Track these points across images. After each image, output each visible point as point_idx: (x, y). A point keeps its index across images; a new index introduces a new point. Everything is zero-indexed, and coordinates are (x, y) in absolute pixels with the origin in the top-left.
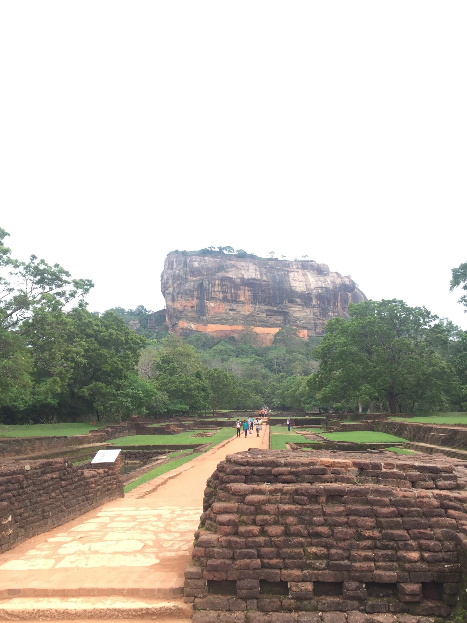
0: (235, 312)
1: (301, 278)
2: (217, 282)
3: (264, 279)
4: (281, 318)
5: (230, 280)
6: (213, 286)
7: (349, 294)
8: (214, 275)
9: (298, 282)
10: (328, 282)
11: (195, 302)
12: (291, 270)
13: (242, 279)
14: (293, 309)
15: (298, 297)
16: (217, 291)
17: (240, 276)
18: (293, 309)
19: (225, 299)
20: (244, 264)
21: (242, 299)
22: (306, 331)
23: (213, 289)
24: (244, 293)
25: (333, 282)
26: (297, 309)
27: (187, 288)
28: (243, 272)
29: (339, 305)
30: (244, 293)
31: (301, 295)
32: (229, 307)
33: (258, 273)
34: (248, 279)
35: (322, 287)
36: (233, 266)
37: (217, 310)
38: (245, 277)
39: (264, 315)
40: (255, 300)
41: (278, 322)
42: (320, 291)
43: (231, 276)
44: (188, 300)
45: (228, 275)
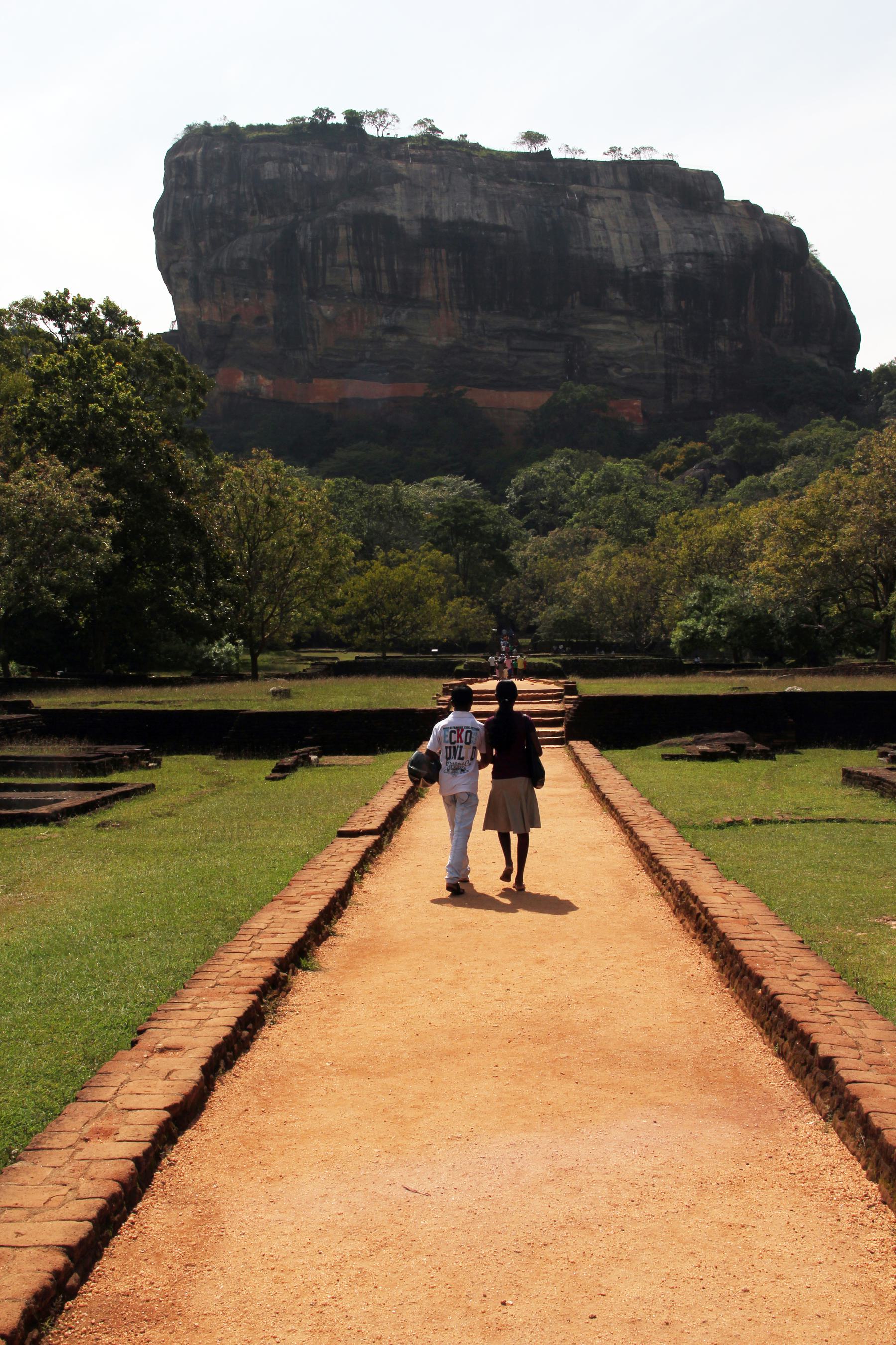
0: (404, 338)
3: (501, 222)
5: (389, 224)
7: (787, 277)
9: (617, 235)
12: (593, 192)
13: (428, 223)
14: (600, 327)
17: (422, 211)
18: (600, 327)
21: (428, 292)
22: (637, 403)
23: (329, 256)
24: (435, 271)
25: (732, 236)
26: (611, 327)
27: (241, 254)
30: (435, 271)
32: (385, 321)
34: (449, 224)
35: (696, 253)
36: (397, 178)
41: (545, 372)
42: (689, 265)
43: (389, 212)
44: (246, 296)
45: (378, 208)
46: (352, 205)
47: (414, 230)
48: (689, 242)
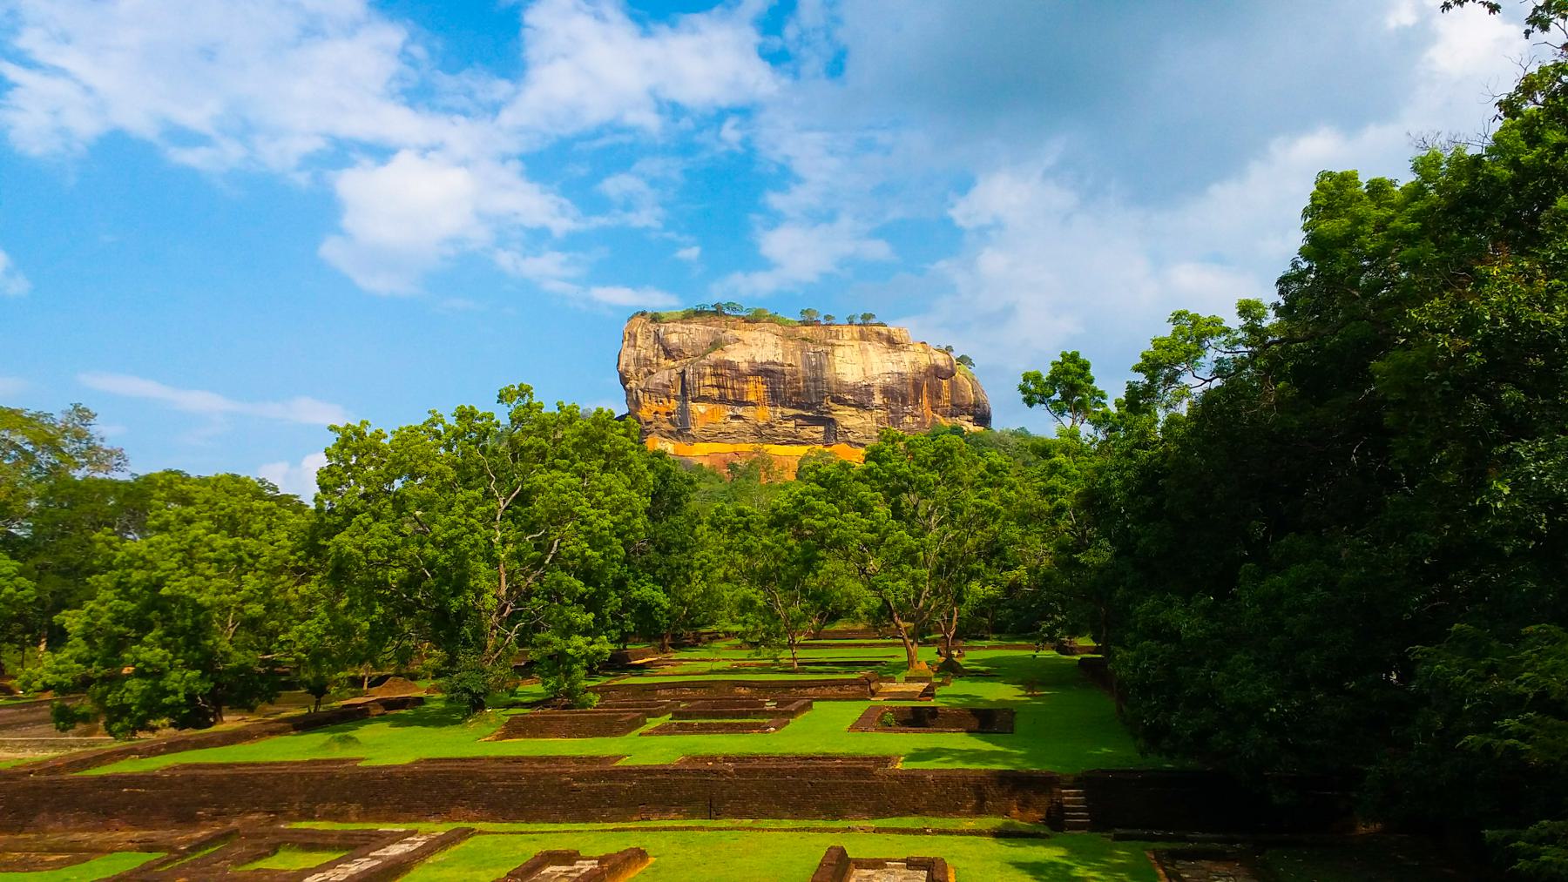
1: (857, 358)
2: (708, 370)
4: (822, 429)
5: (730, 365)
6: (702, 376)
8: (704, 356)
10: (907, 363)
11: (674, 405)
13: (752, 363)
15: (849, 393)
16: (707, 385)
17: (749, 358)
19: (722, 400)
20: (757, 334)
21: (752, 398)
28: (753, 350)
29: (925, 401)
31: (854, 389)
33: (780, 351)
37: (709, 419)
38: (758, 359)
39: (792, 424)
40: (775, 398)
46: (715, 356)
47: (744, 367)
48: (890, 367)
